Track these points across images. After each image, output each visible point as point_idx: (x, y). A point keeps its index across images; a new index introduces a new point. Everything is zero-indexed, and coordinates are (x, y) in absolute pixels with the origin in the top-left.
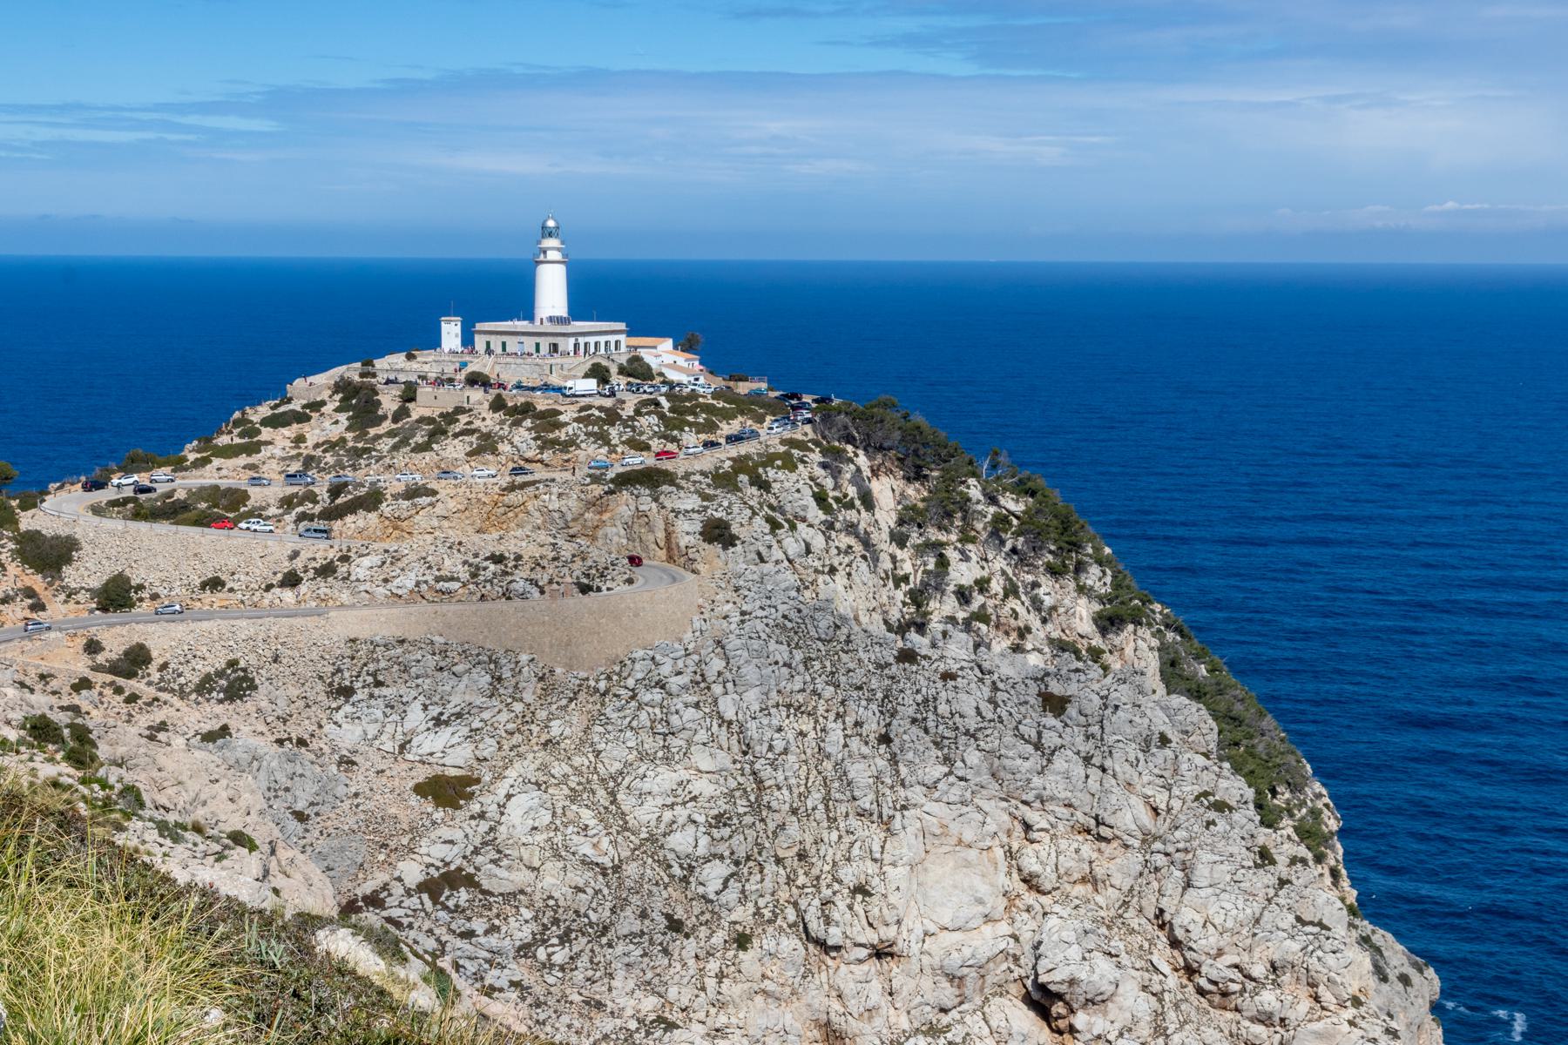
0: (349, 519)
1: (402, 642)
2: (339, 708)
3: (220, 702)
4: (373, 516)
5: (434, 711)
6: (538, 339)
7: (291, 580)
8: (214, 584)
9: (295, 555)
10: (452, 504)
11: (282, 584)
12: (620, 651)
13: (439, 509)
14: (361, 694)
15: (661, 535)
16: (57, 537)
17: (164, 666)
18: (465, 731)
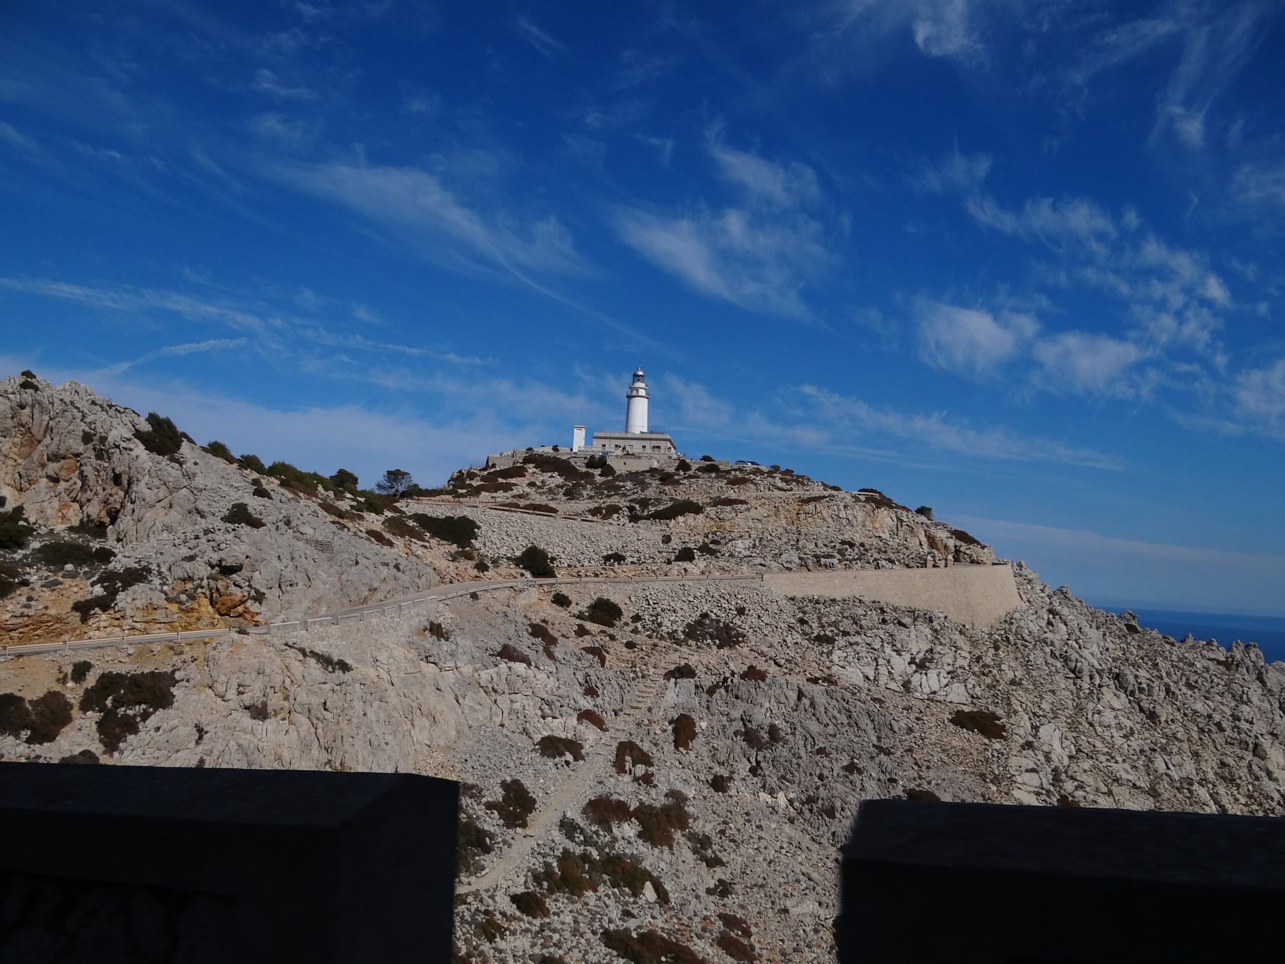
0: (680, 519)
1: (834, 601)
2: (830, 653)
3: (720, 647)
4: (701, 516)
5: (908, 657)
6: (644, 443)
7: (686, 555)
8: (618, 558)
9: (667, 539)
10: (762, 512)
11: (678, 559)
12: (1002, 613)
13: (753, 513)
14: (841, 641)
15: (924, 540)
16: (448, 518)
17: (637, 618)
18: (944, 674)
